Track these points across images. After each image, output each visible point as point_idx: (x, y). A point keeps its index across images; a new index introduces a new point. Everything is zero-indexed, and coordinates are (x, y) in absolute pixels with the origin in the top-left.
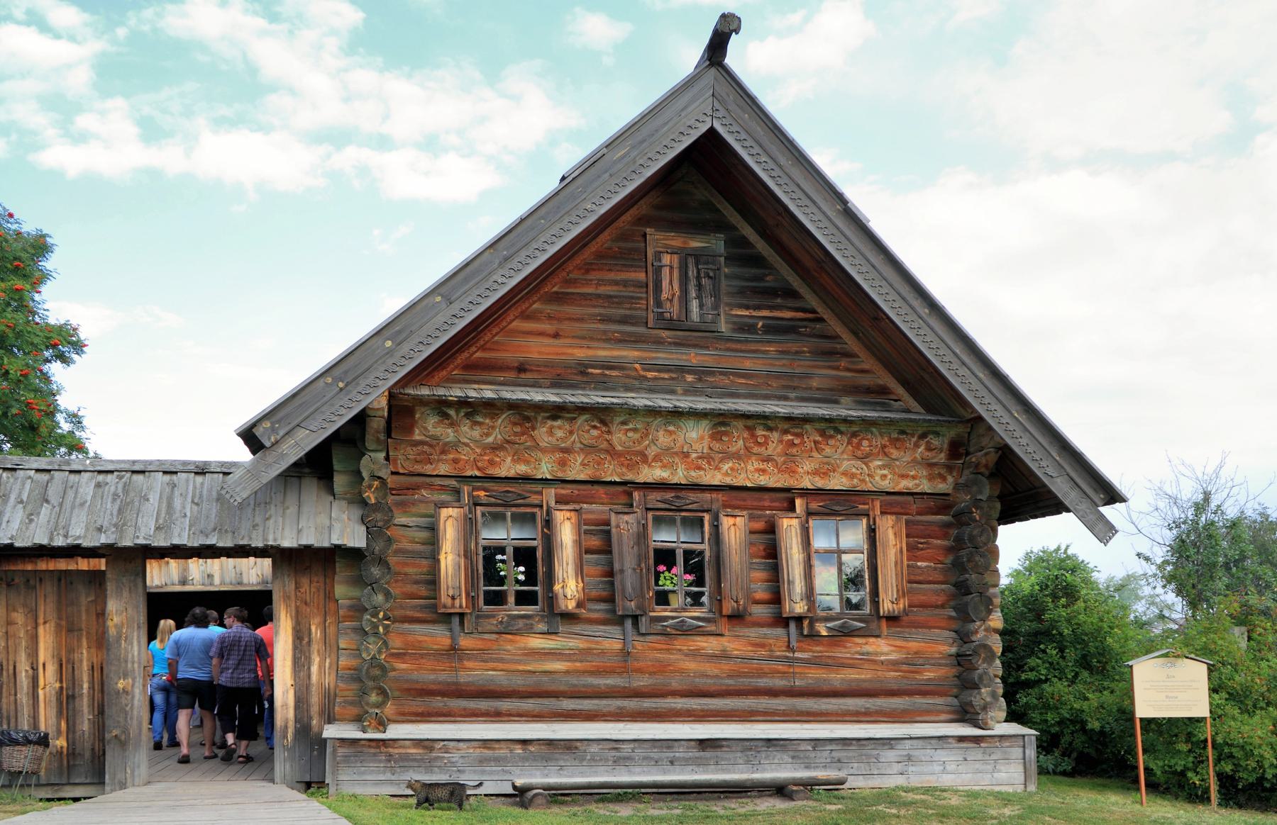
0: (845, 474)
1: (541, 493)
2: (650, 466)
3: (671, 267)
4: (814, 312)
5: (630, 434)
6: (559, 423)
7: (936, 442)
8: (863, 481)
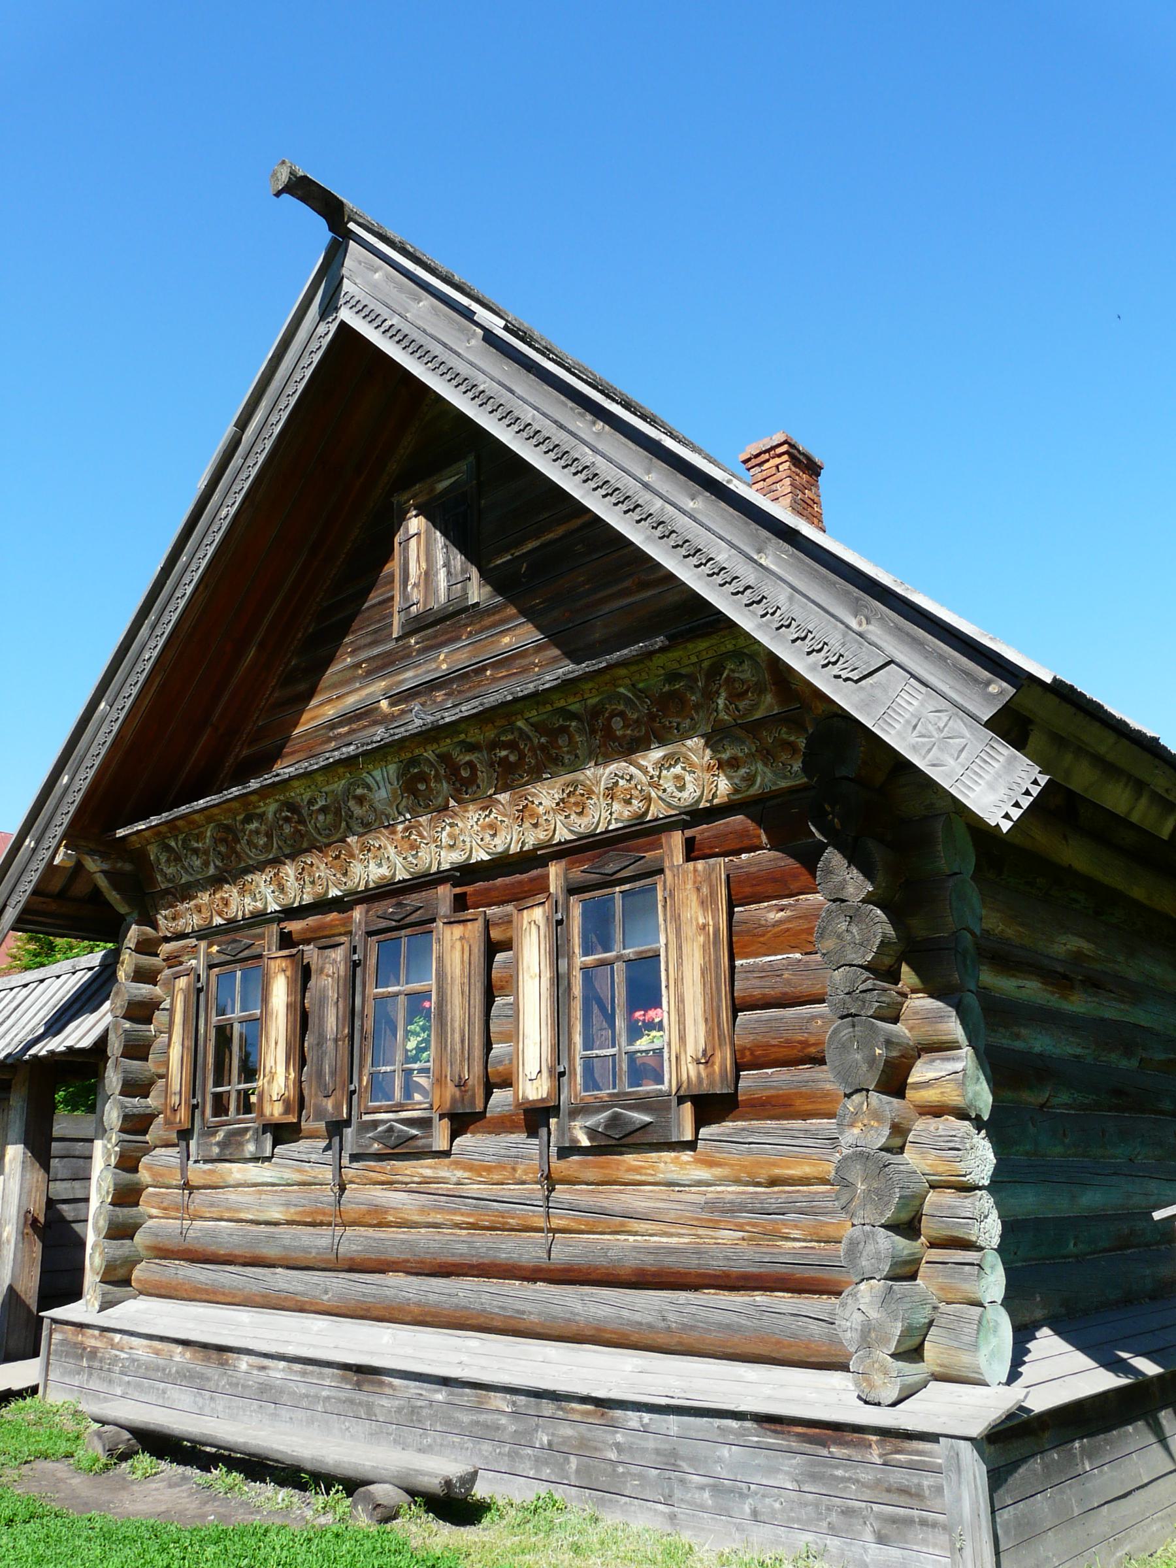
0: (611, 793)
6: (254, 826)
7: (746, 673)
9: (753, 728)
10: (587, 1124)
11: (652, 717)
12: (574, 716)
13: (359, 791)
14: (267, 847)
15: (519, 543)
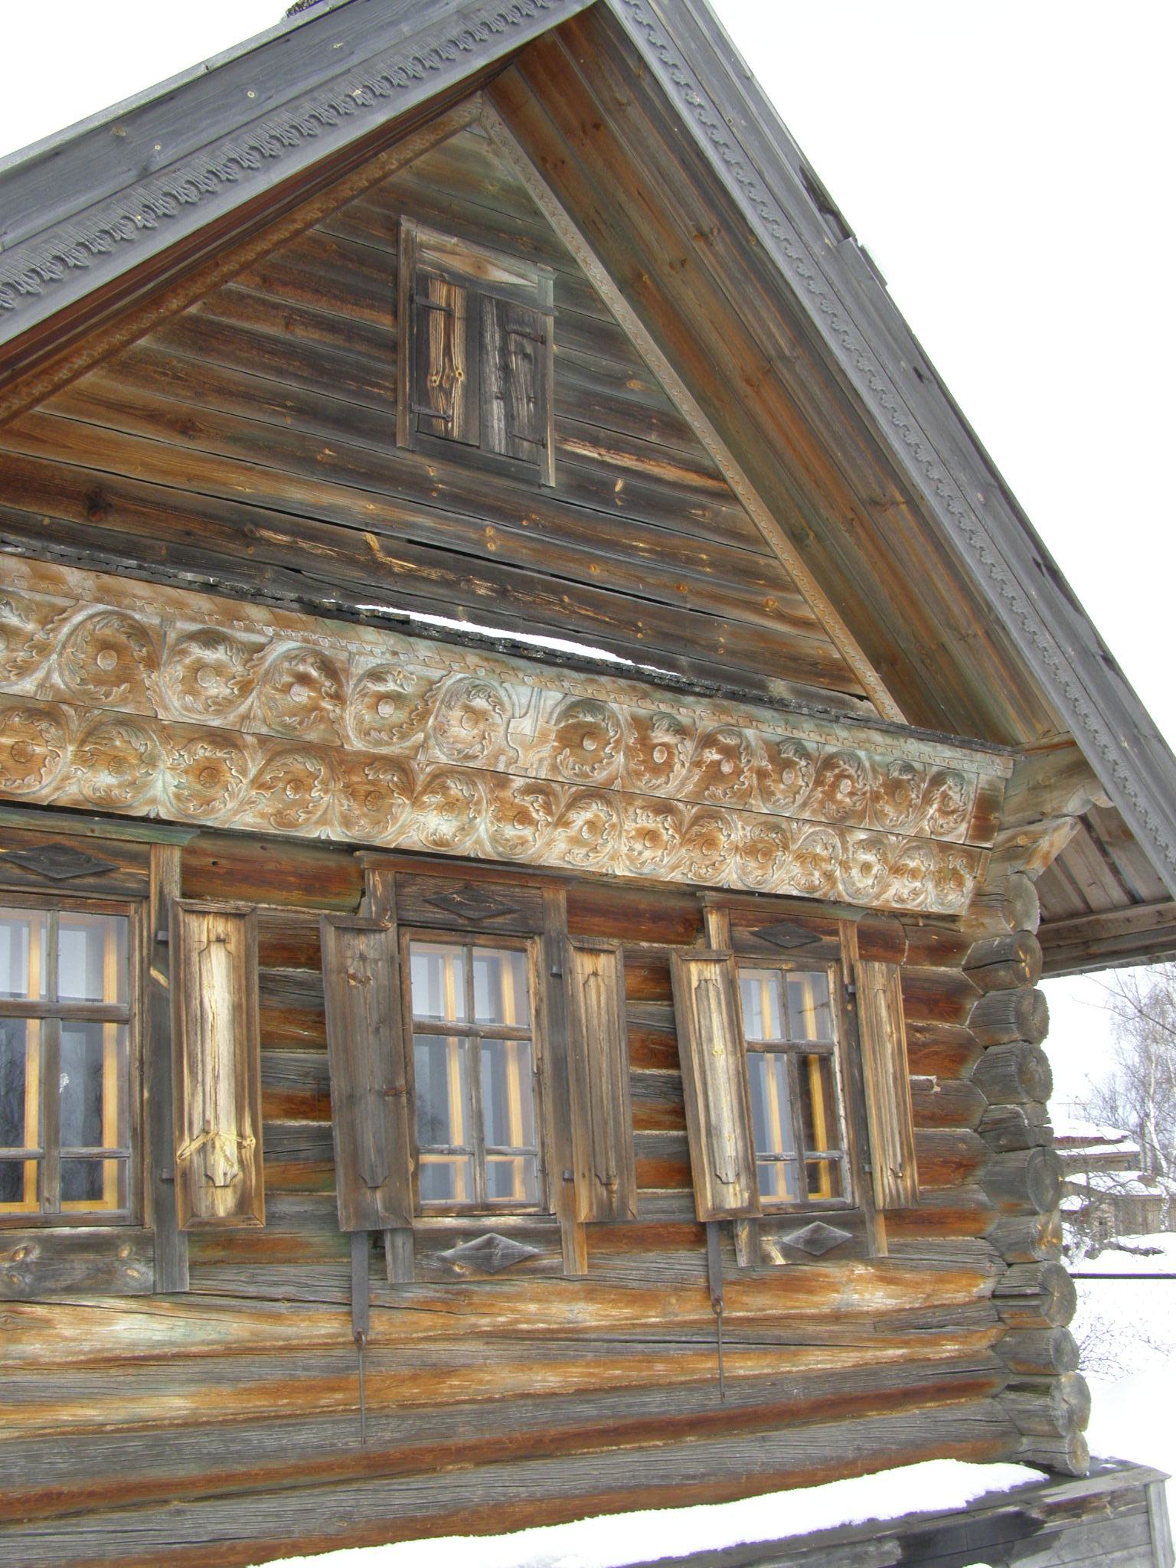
1: (143, 860)
2: (416, 802)
3: (449, 315)
4: (717, 476)
5: (386, 710)
8: (829, 876)
9: (946, 848)
10: (787, 1239)
11: (876, 797)
12: (803, 753)
13: (480, 703)
14: (222, 706)
15: (615, 447)
